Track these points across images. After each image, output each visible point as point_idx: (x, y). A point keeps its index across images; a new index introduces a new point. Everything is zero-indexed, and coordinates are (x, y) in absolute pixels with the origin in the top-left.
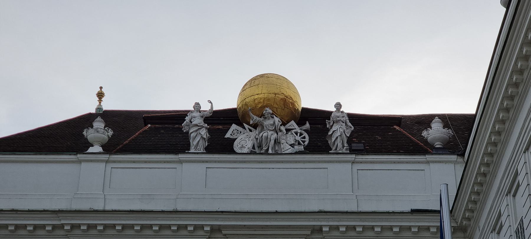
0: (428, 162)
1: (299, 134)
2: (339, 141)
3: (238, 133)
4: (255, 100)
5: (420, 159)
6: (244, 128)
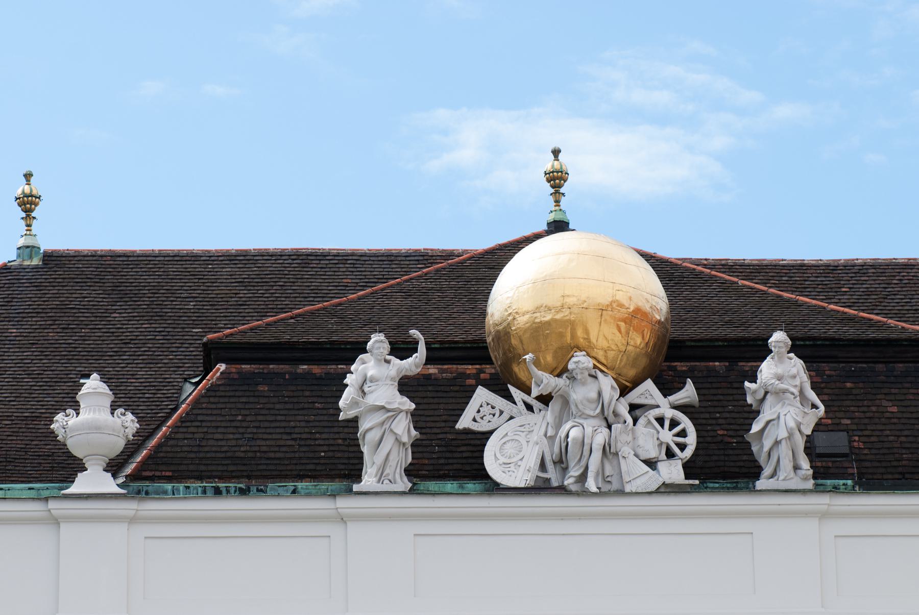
1: (667, 424)
2: (784, 452)
3: (494, 415)
6: (509, 397)
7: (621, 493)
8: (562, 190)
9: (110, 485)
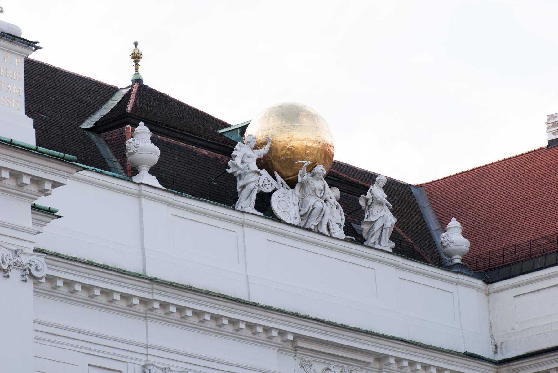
0: (457, 283)
4: (307, 148)
5: (479, 284)
7: (331, 237)
8: (139, 63)
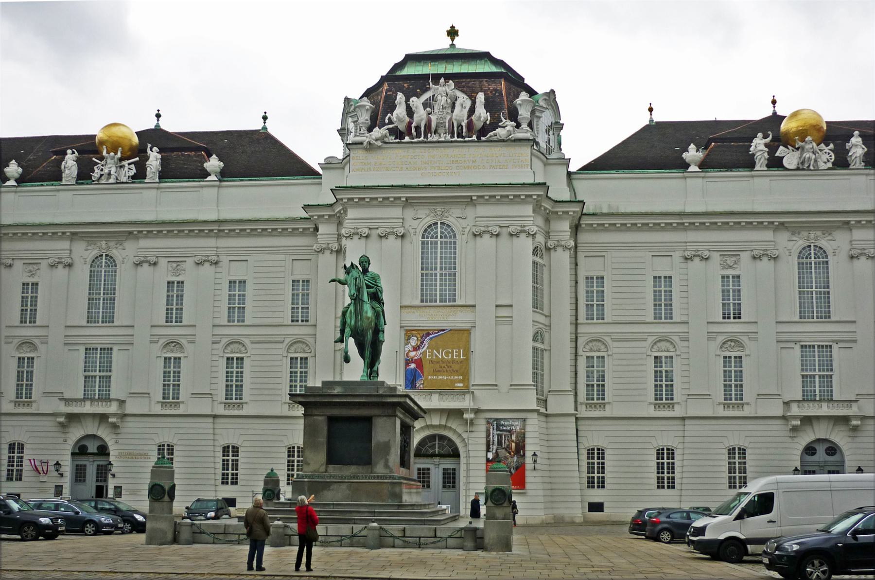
2: (858, 159)
6: (788, 148)
9: (697, 169)
